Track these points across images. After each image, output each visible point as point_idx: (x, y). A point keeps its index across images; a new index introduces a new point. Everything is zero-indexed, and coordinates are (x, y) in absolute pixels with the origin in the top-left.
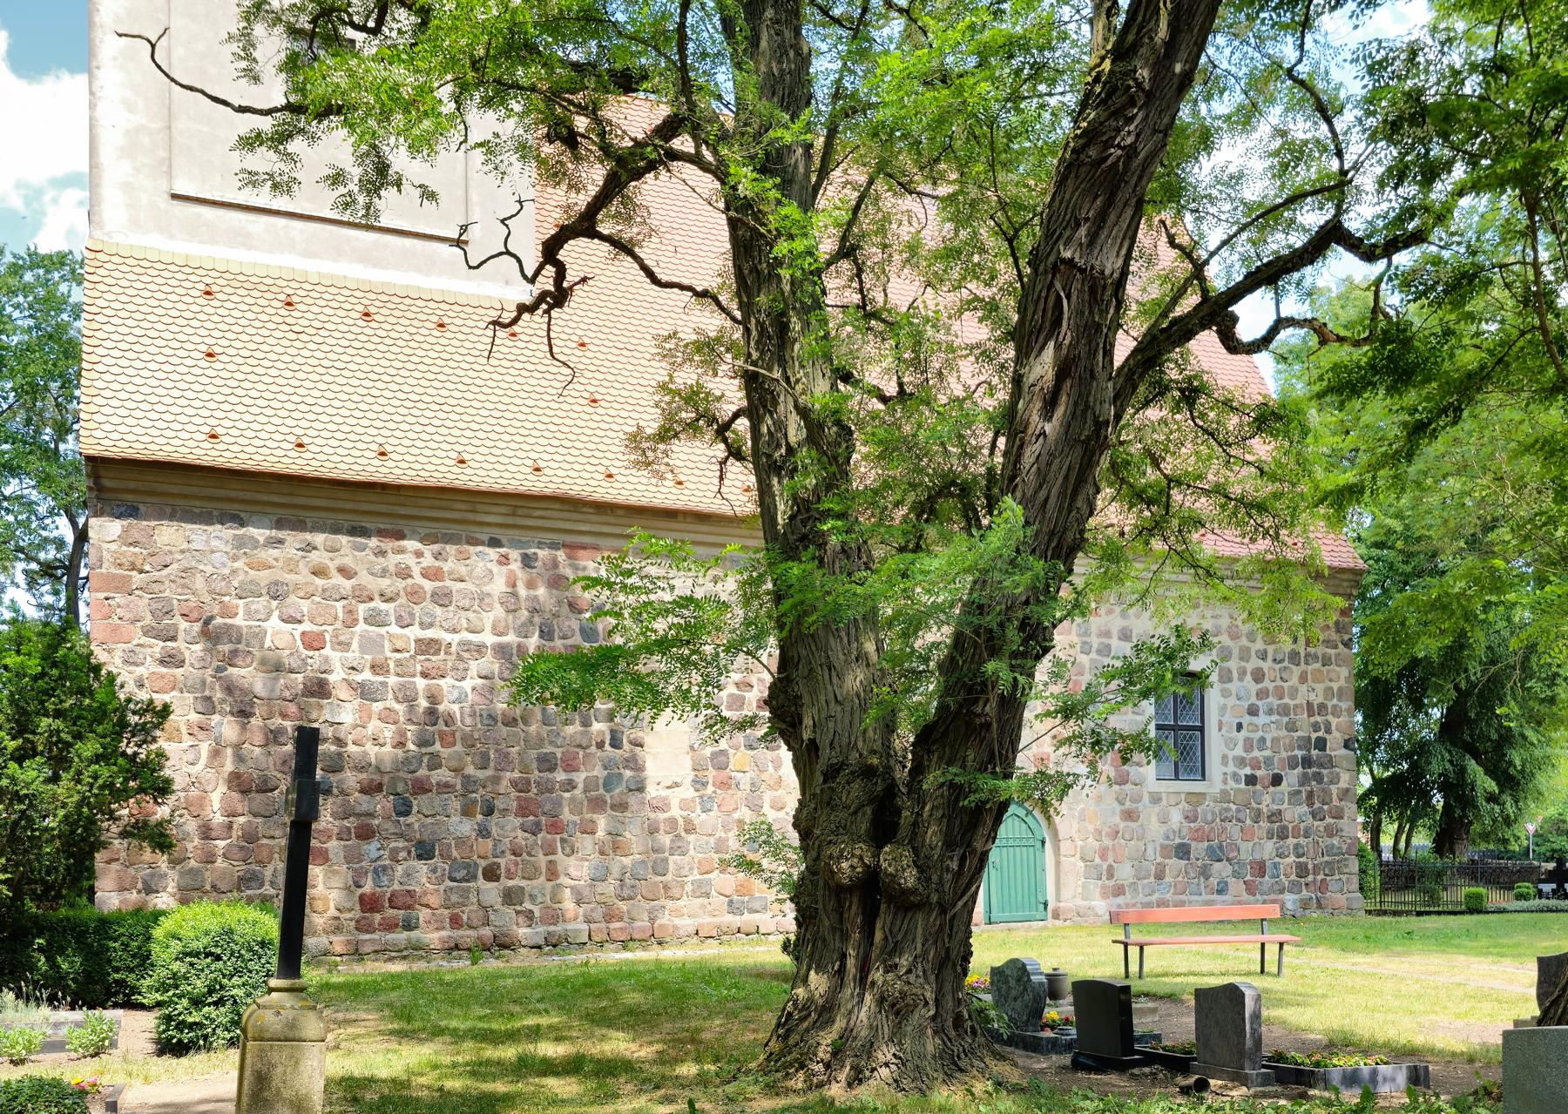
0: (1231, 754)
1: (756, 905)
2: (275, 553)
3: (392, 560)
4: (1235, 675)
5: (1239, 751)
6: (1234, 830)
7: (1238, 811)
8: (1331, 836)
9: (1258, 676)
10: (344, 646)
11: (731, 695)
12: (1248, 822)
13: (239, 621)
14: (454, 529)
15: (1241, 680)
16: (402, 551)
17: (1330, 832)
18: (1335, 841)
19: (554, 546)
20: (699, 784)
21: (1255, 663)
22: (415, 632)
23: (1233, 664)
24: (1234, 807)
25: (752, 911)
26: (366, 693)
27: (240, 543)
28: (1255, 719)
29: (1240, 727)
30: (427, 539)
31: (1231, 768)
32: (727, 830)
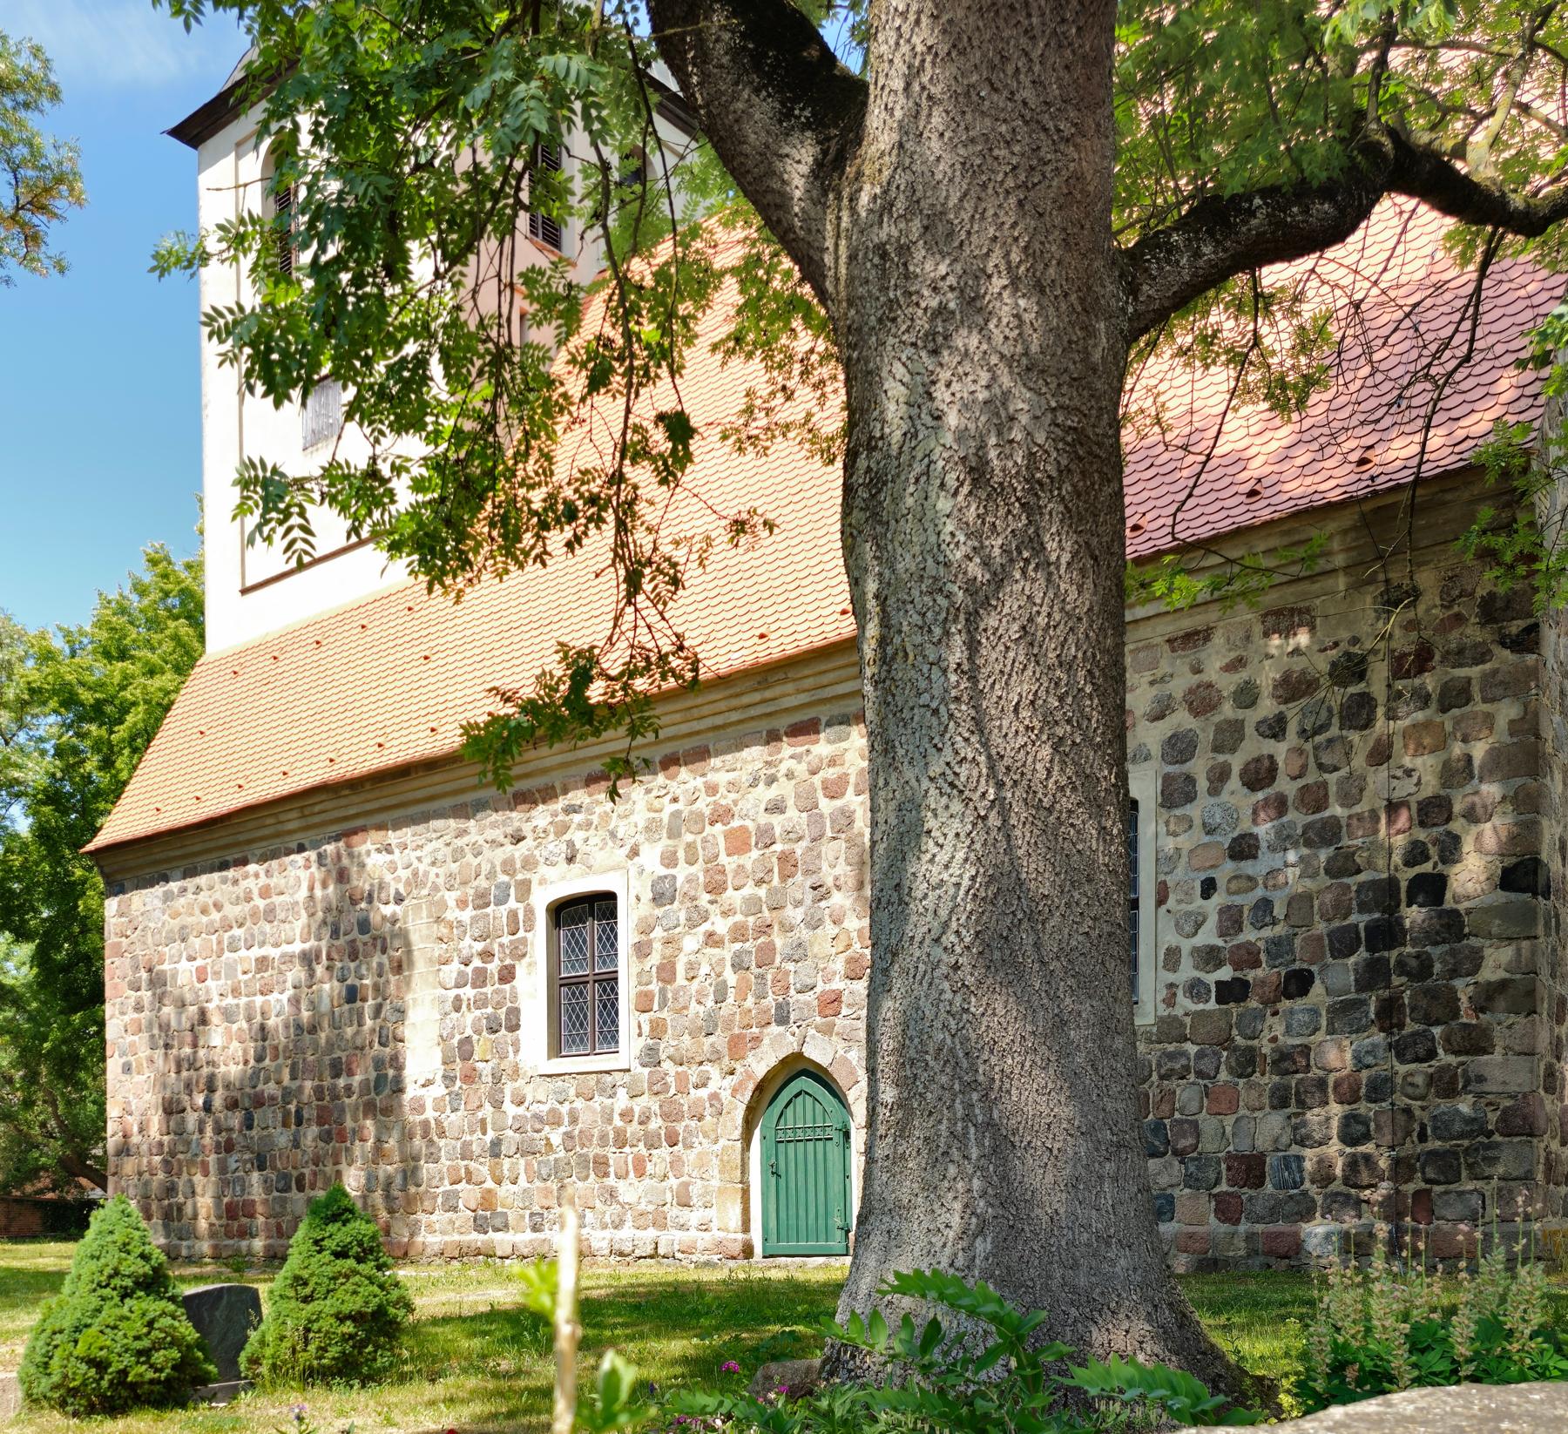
0: (1186, 945)
1: (498, 1222)
2: (182, 900)
3: (244, 884)
4: (1202, 784)
5: (1208, 936)
6: (1186, 1094)
7: (1200, 1055)
8: (1450, 1091)
9: (1259, 776)
10: (217, 974)
11: (476, 970)
12: (1224, 1076)
13: (166, 967)
14: (276, 844)
15: (1214, 791)
16: (246, 877)
17: (1446, 1085)
18: (1465, 1106)
19: (337, 839)
20: (449, 1079)
21: (1253, 746)
22: (256, 952)
23: (1199, 767)
24: (1192, 1049)
25: (497, 1230)
26: (228, 1015)
27: (168, 897)
28: (1248, 867)
29: (1209, 888)
30: (263, 859)
31: (1188, 971)
32: (472, 1132)
